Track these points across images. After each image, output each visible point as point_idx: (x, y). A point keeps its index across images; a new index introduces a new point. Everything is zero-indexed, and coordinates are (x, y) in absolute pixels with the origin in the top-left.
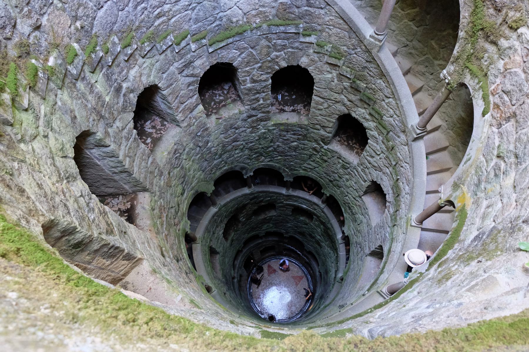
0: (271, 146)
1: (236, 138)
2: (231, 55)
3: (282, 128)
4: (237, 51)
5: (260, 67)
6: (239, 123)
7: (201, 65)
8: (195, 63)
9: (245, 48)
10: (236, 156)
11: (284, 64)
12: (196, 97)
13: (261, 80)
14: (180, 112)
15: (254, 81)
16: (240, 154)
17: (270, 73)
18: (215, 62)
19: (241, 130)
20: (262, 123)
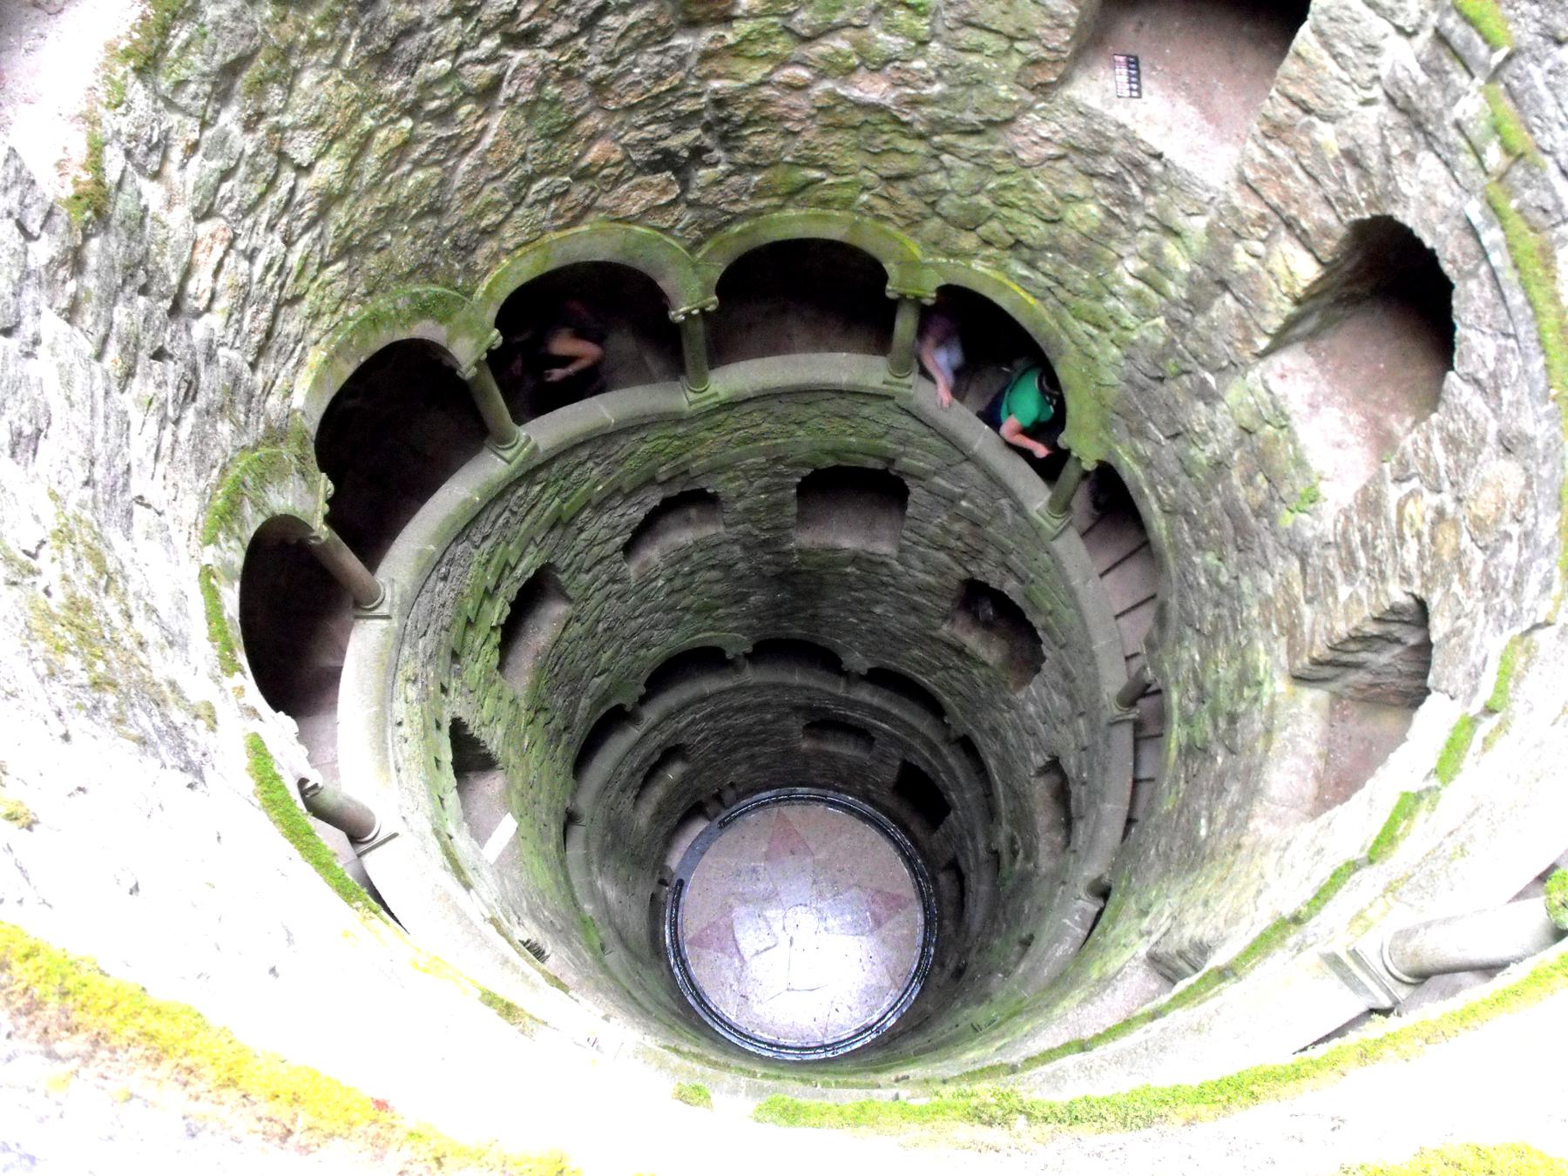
0: (1216, 727)
1: (1244, 520)
2: (1475, 339)
3: (1260, 746)
4: (1491, 366)
5: (1440, 513)
6: (1286, 520)
7: (1429, 202)
8: (1432, 155)
9: (1497, 389)
10: (1197, 560)
11: (1439, 627)
12: (1331, 219)
13: (1401, 537)
14: (1270, 155)
15: (1401, 508)
16: (1203, 581)
17: (1423, 574)
18: (1447, 268)
19: (1270, 541)
20: (1283, 640)
